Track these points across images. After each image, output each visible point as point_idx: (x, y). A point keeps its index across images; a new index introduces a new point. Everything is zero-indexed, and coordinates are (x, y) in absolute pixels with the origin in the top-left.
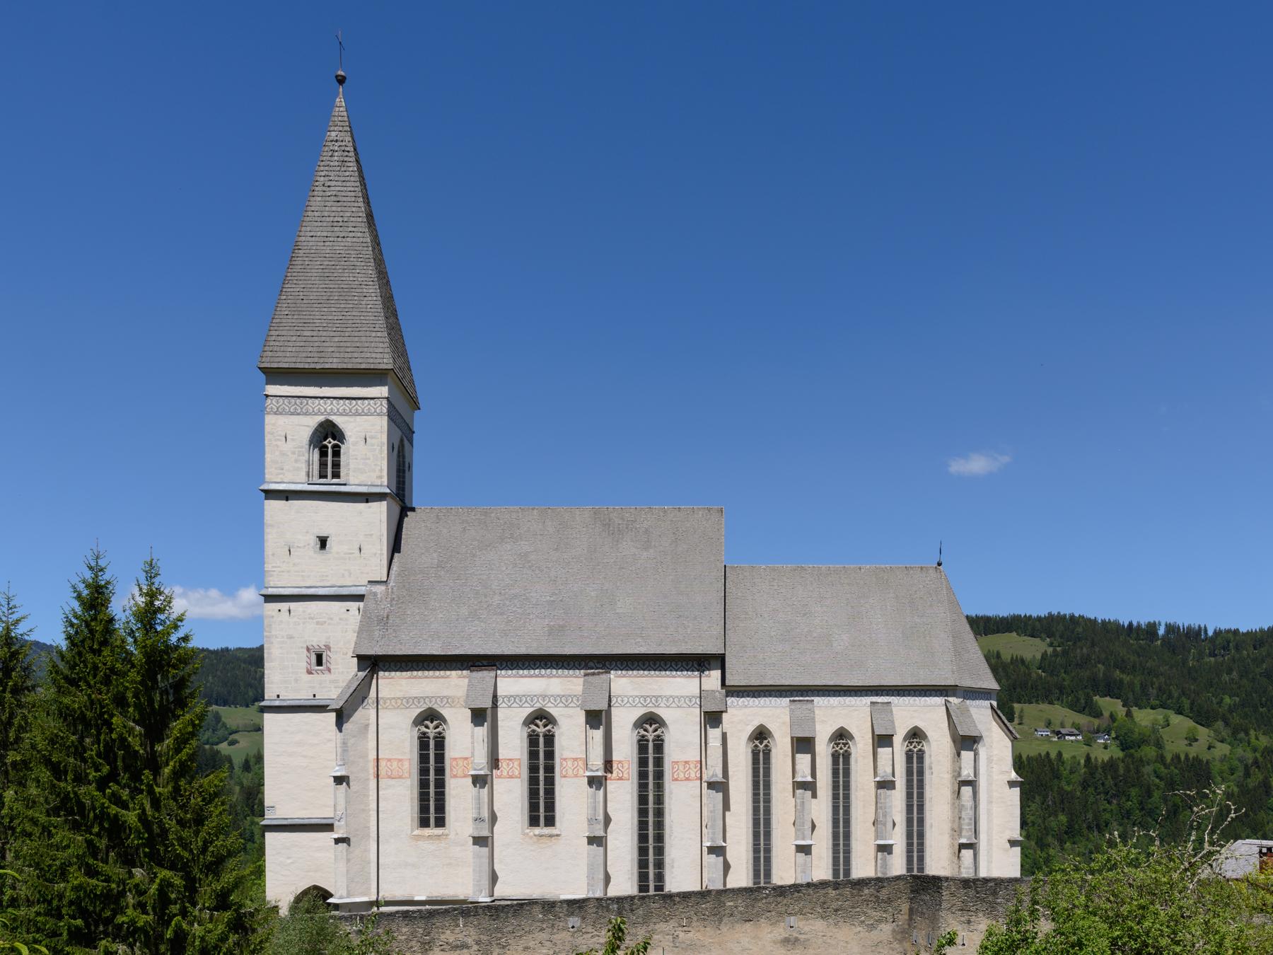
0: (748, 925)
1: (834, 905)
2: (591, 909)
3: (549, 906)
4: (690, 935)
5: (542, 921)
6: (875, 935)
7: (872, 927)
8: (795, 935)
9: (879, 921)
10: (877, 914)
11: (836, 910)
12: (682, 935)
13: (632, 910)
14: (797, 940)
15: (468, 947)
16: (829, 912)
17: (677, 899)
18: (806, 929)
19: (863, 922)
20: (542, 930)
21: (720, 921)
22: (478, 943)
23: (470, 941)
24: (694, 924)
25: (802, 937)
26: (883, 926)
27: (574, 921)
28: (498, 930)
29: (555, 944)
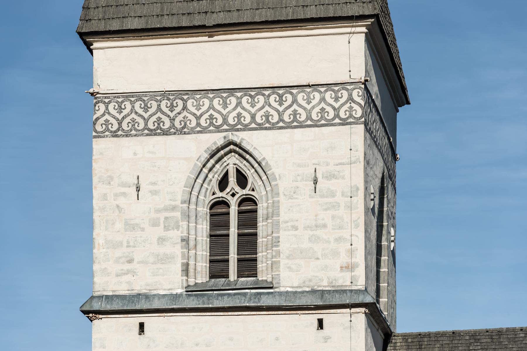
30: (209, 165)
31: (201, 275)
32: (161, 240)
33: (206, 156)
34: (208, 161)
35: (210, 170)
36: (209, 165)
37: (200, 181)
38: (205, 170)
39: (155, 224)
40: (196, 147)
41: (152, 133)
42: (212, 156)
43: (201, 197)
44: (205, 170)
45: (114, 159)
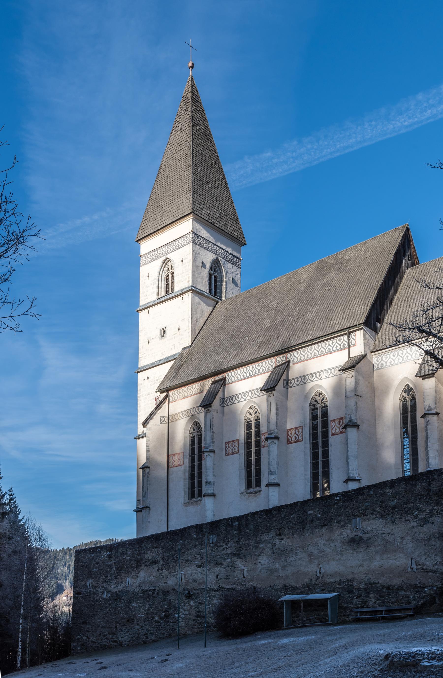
0: (323, 530)
1: (393, 503)
2: (223, 527)
3: (199, 528)
4: (283, 542)
5: (196, 539)
6: (427, 529)
7: (424, 522)
8: (360, 534)
9: (431, 514)
10: (427, 508)
11: (393, 508)
12: (277, 542)
13: (247, 525)
14: (361, 538)
15: (158, 563)
16: (389, 512)
17: (275, 513)
18: (369, 528)
19: (416, 517)
20: (196, 546)
21: (304, 528)
22: (163, 559)
23: (159, 558)
24: (286, 532)
25: (365, 536)
26: (432, 519)
27: (213, 538)
28: (173, 549)
29: (202, 557)
30: (164, 266)
31: (163, 293)
32: (153, 288)
33: (161, 263)
34: (163, 265)
35: (164, 267)
36: (164, 266)
37: (162, 270)
38: (163, 268)
39: (151, 284)
40: (159, 262)
41: (151, 261)
42: (164, 263)
43: (163, 275)
44: (163, 268)
45: (144, 270)
